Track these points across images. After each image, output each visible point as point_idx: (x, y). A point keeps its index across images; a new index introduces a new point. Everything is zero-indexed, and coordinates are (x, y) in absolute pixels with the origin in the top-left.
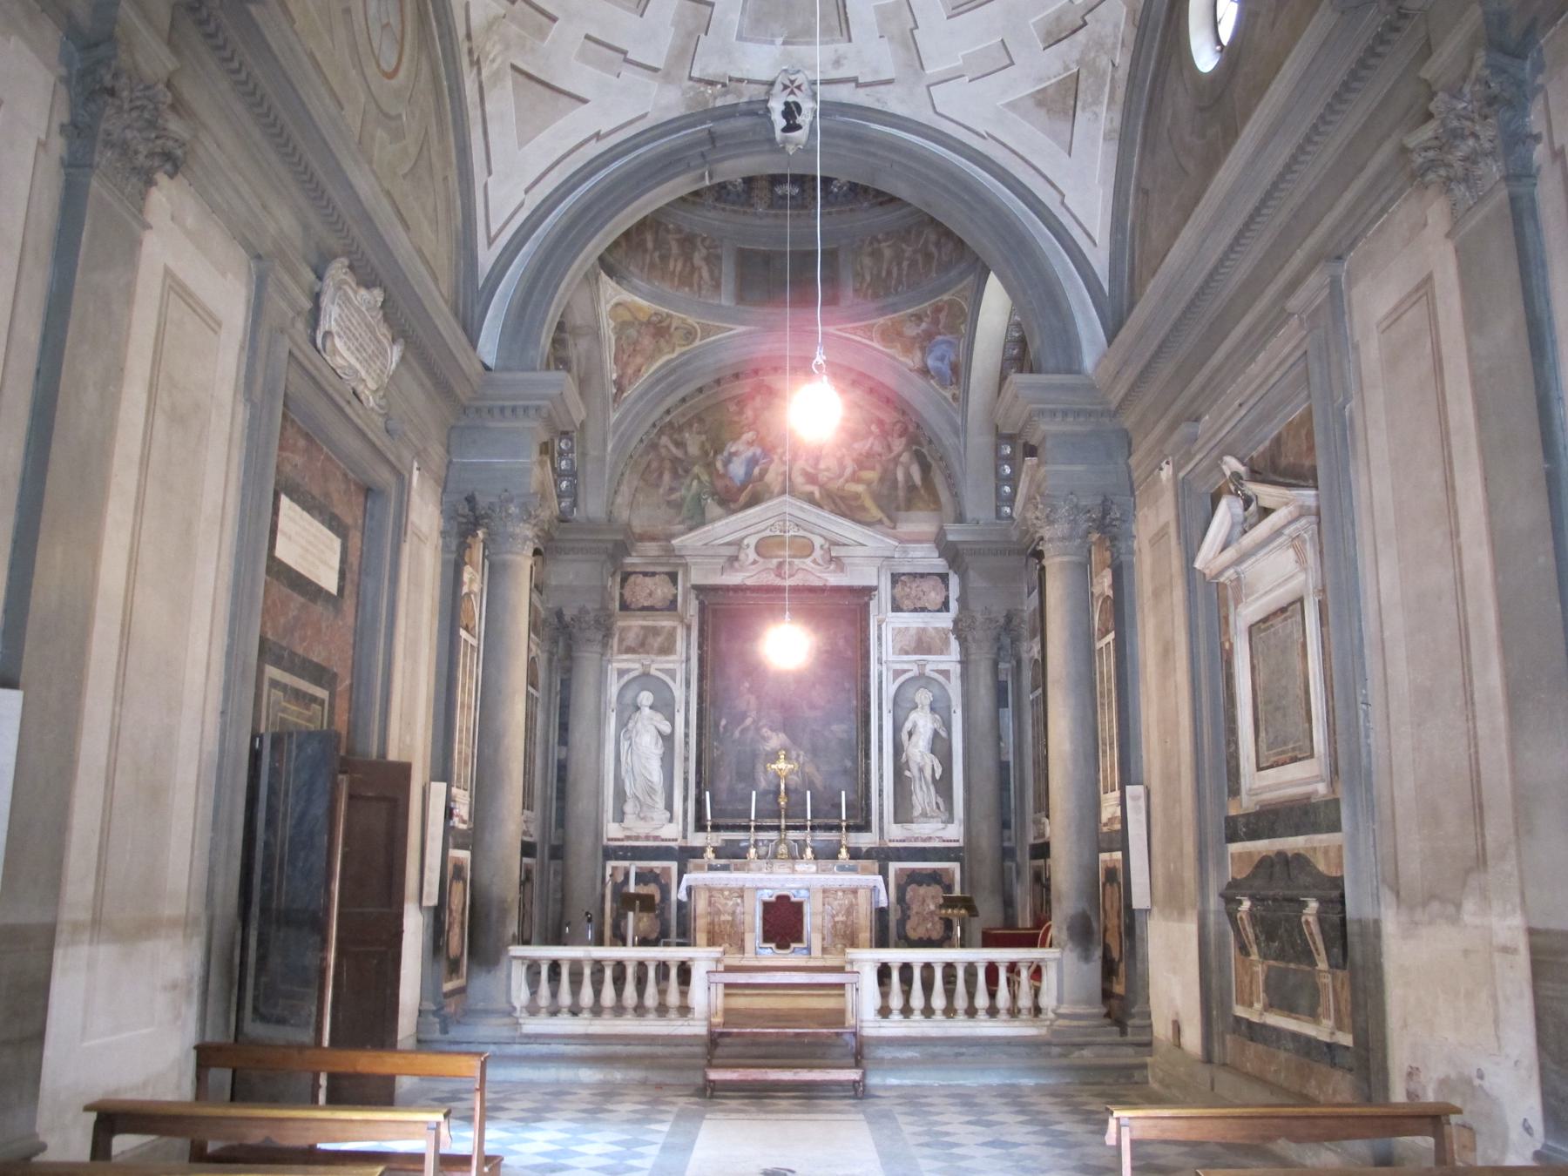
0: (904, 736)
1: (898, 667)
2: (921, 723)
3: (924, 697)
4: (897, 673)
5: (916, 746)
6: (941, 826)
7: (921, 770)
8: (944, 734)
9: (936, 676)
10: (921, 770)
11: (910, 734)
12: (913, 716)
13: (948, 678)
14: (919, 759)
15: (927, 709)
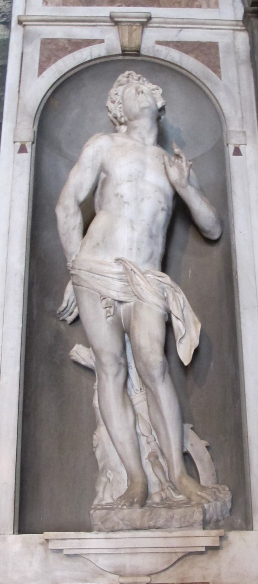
0: (67, 217)
1: (59, 32)
2: (122, 168)
3: (135, 94)
4: (52, 51)
5: (105, 244)
6: (203, 538)
7: (124, 331)
8: (203, 211)
9: (175, 56)
10: (124, 331)
11: (88, 211)
12: (97, 149)
13: (216, 68)
14: (115, 289)
15: (145, 129)
